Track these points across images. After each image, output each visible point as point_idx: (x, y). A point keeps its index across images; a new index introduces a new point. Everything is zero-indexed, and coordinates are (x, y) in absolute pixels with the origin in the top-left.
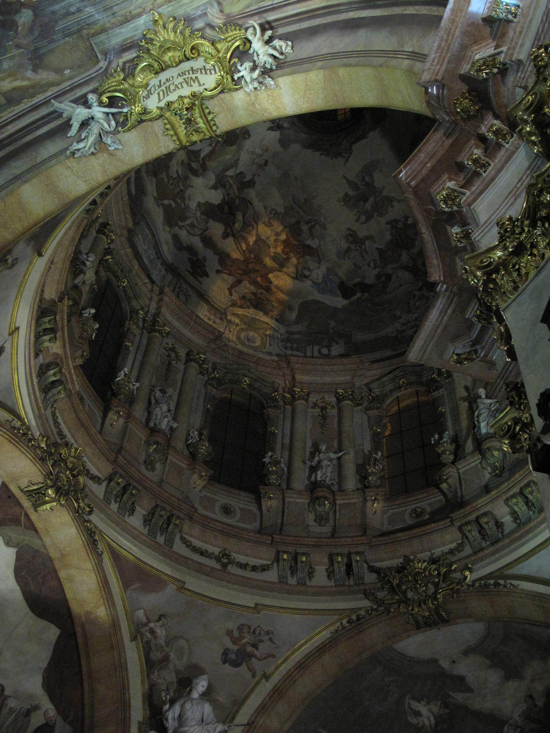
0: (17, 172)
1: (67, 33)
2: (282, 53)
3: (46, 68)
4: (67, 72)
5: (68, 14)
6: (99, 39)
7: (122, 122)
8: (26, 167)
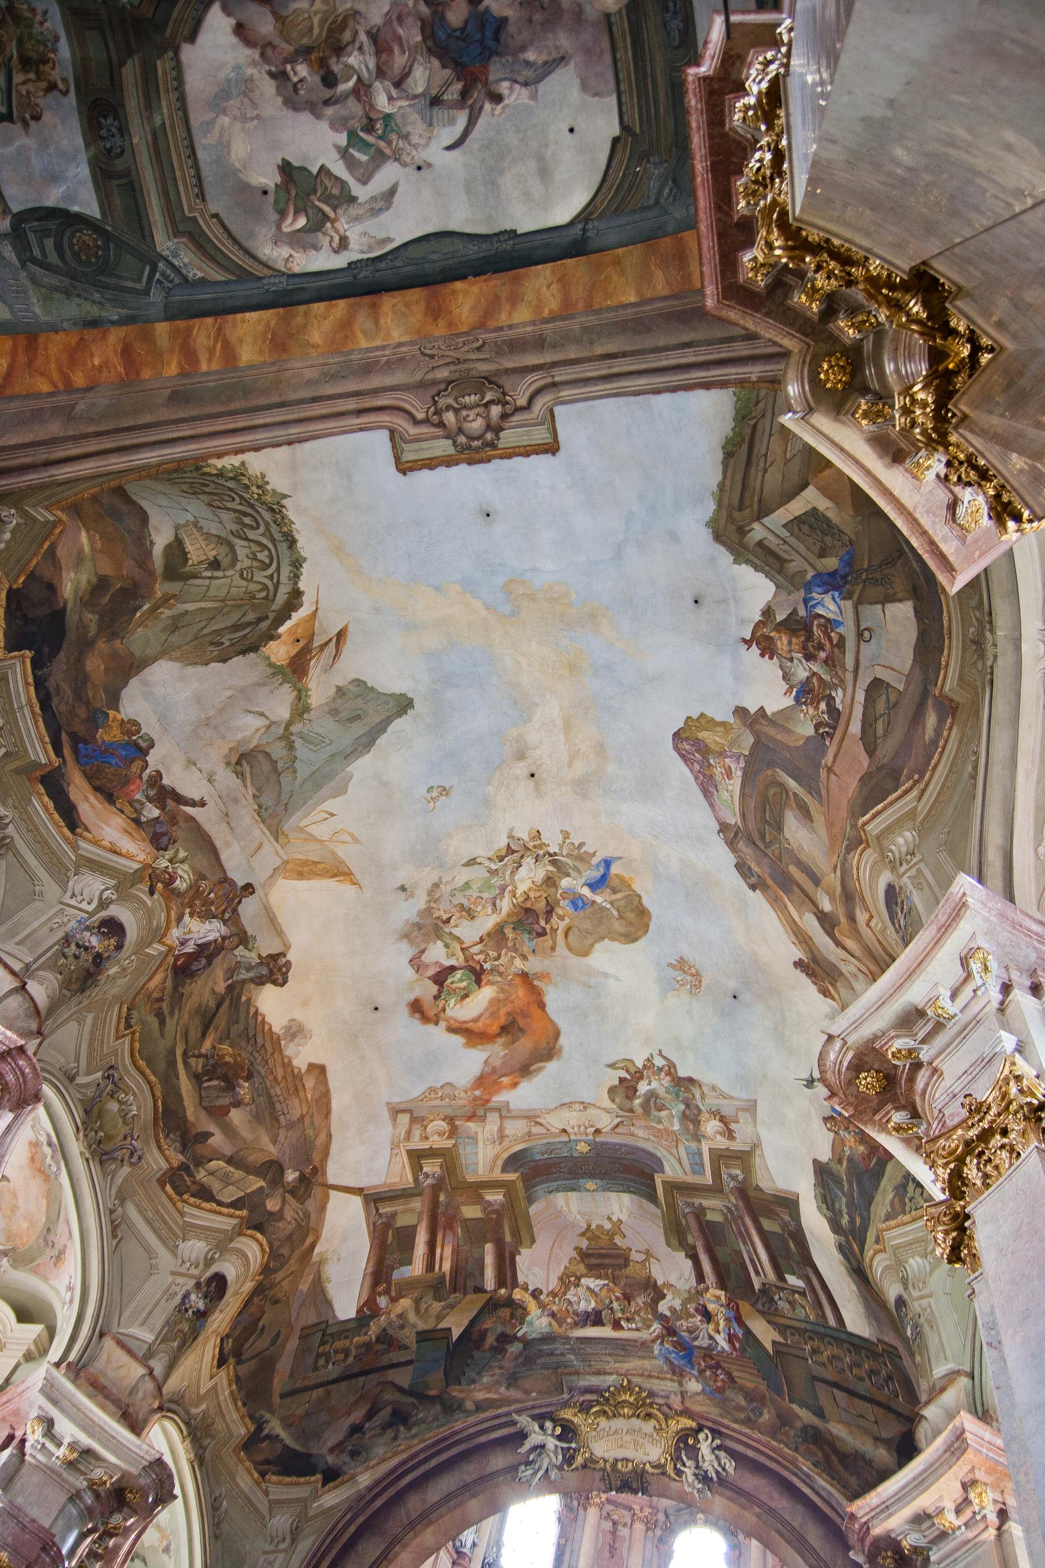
0: (469, 1479)
1: (544, 1366)
2: (724, 1469)
3: (518, 1388)
4: (534, 1394)
5: (552, 1354)
6: (569, 1378)
7: (569, 1460)
8: (475, 1476)
